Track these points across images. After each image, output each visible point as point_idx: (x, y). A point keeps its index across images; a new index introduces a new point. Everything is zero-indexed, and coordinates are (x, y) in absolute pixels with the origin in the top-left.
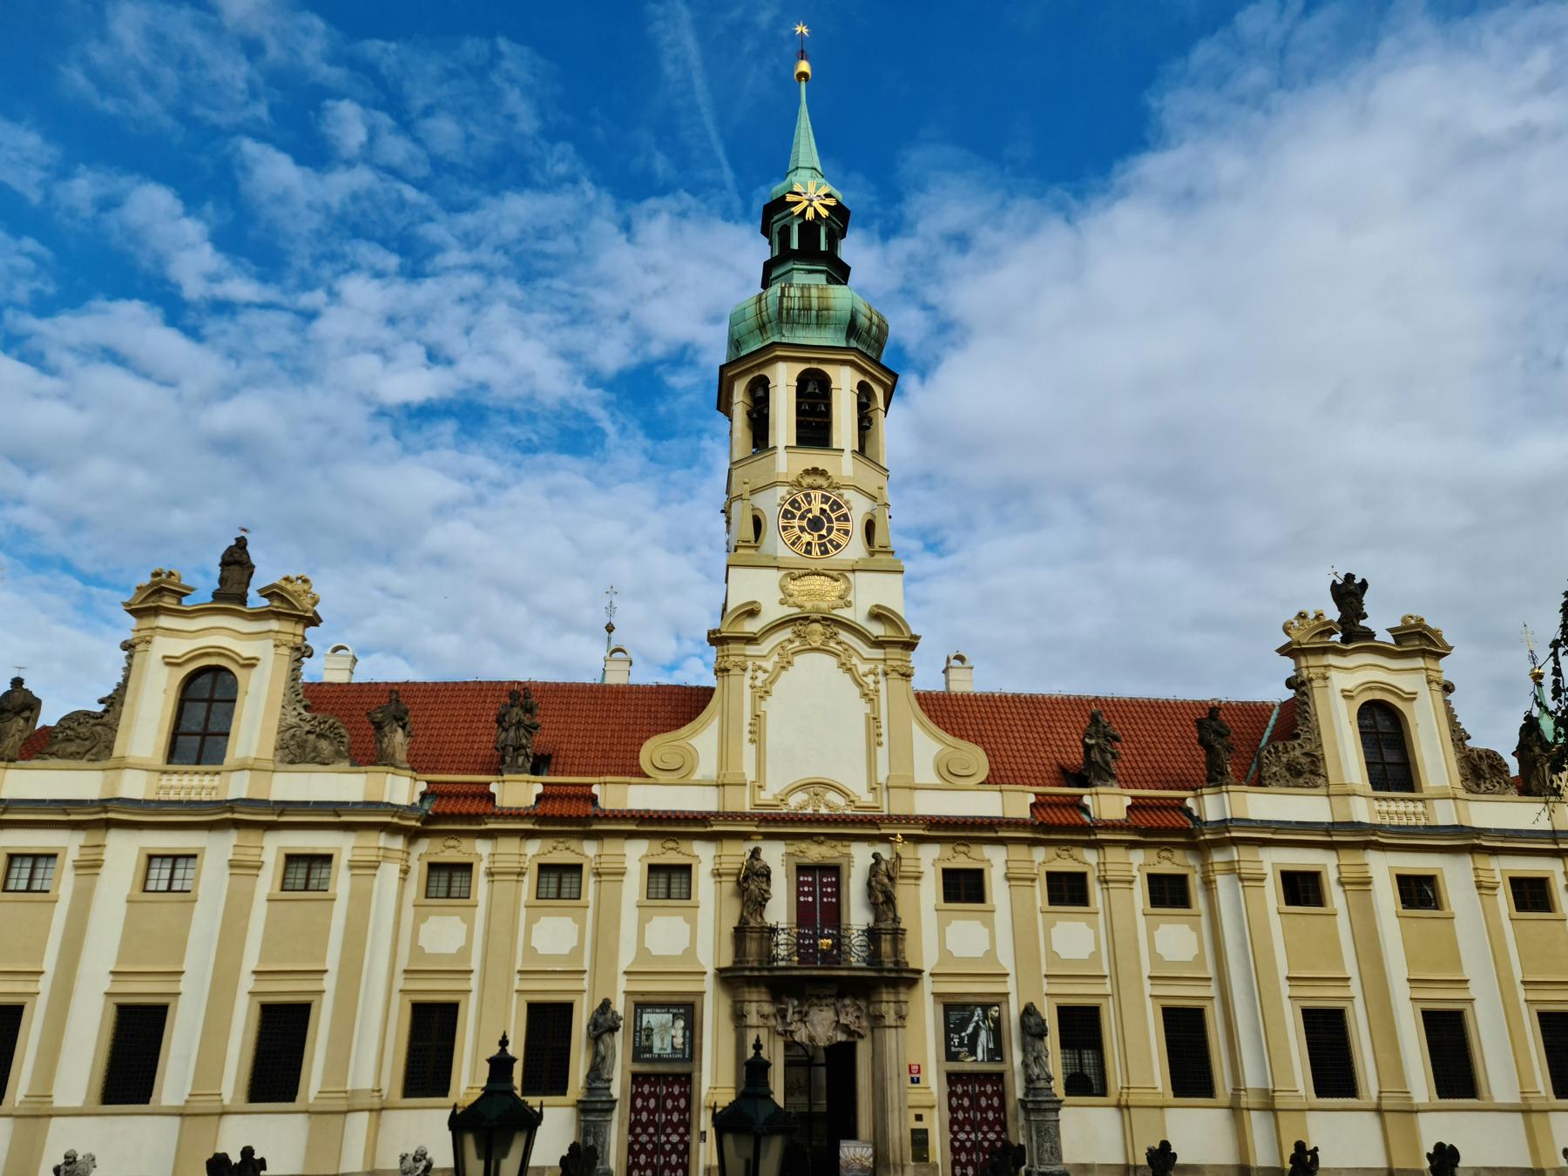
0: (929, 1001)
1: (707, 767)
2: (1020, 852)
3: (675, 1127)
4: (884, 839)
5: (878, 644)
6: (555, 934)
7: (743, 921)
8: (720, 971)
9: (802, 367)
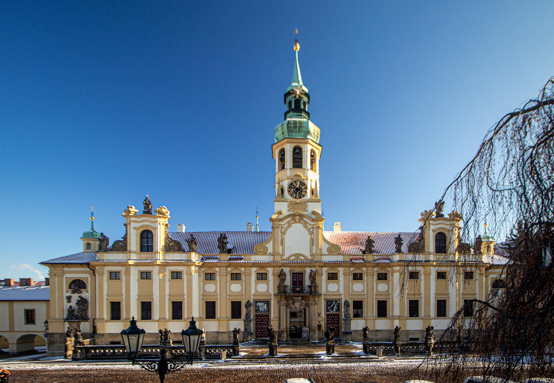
0: (323, 301)
1: (270, 250)
2: (348, 268)
3: (266, 325)
4: (314, 266)
5: (313, 220)
6: (236, 287)
7: (280, 284)
8: (274, 295)
9: (294, 145)
